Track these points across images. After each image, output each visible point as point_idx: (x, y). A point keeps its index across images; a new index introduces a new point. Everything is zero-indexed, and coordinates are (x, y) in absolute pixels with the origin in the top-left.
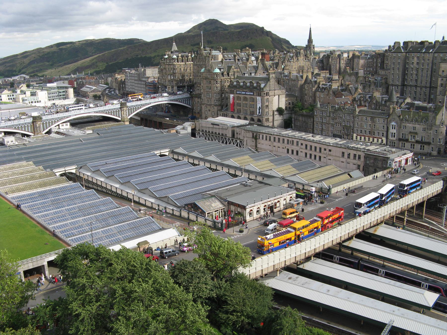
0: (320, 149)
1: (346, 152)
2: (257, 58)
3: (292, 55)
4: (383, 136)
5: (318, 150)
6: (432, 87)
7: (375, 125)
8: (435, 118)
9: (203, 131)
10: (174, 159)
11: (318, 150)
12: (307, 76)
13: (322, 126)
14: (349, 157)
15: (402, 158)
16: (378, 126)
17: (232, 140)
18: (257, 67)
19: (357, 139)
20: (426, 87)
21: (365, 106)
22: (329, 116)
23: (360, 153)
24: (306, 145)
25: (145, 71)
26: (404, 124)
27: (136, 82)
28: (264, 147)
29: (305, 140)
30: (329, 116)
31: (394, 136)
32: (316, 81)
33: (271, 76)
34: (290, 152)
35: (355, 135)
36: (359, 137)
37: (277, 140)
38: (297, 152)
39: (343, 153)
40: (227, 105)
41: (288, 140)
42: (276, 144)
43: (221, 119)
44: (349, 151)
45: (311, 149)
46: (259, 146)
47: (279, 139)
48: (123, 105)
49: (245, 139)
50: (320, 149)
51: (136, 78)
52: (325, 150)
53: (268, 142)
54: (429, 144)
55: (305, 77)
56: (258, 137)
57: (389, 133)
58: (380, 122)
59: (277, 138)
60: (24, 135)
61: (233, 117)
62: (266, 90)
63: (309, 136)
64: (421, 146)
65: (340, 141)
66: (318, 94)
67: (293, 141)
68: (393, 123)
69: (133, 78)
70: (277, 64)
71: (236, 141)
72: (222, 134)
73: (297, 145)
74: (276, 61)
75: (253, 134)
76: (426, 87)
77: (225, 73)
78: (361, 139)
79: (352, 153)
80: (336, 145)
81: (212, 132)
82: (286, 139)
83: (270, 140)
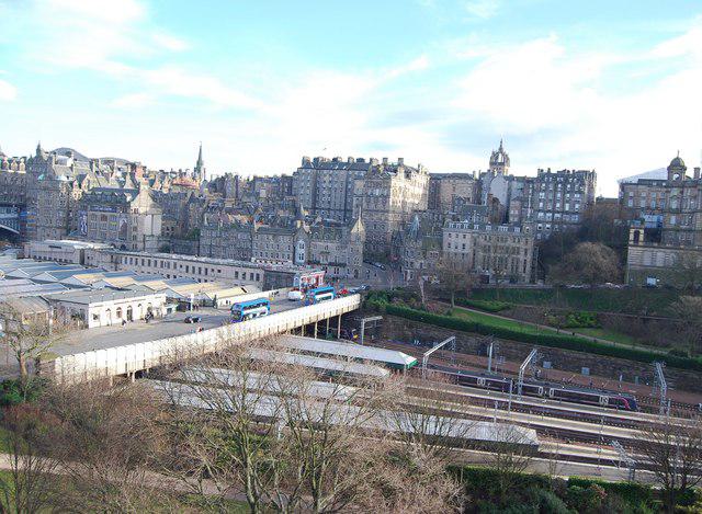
2: (124, 175)
3: (174, 176)
5: (203, 272)
6: (347, 210)
8: (349, 233)
11: (203, 272)
15: (313, 275)
18: (124, 182)
20: (340, 210)
37: (146, 263)
39: (237, 273)
42: (145, 268)
44: (245, 270)
45: (194, 272)
54: (344, 265)
58: (285, 241)
62: (134, 206)
73: (175, 267)
74: (152, 178)
76: (340, 210)
77: (76, 183)
79: (248, 271)
82: (159, 261)
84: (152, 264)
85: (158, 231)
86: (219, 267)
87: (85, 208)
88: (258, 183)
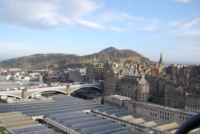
0: (168, 113)
1: (182, 116)
2: (135, 67)
3: (152, 66)
5: (167, 114)
9: (107, 101)
10: (112, 121)
11: (167, 114)
12: (160, 77)
14: (184, 119)
17: (122, 107)
18: (135, 71)
19: (187, 109)
21: (191, 92)
24: (161, 111)
25: (79, 70)
27: (74, 75)
28: (138, 111)
29: (160, 109)
32: (165, 79)
33: (142, 76)
34: (152, 114)
35: (186, 107)
36: (188, 108)
37: (145, 108)
38: (156, 114)
39: (181, 116)
40: (120, 89)
41: (151, 108)
43: (116, 96)
44: (184, 115)
45: (163, 114)
46: (136, 110)
48: (68, 86)
49: (129, 107)
50: (168, 113)
51: (75, 74)
52: (171, 114)
53: (141, 109)
55: (159, 77)
56: (136, 106)
60: (17, 98)
61: (122, 95)
62: (140, 83)
63: (162, 107)
65: (178, 110)
66: (166, 85)
67: (154, 109)
69: (73, 73)
70: (145, 70)
71: (124, 108)
72: (117, 104)
73: (156, 111)
74: (145, 68)
77: (120, 73)
78: (194, 110)
81: (112, 103)
82: (150, 108)
84: (148, 109)
85: (148, 91)
87: (123, 83)
88: (185, 69)
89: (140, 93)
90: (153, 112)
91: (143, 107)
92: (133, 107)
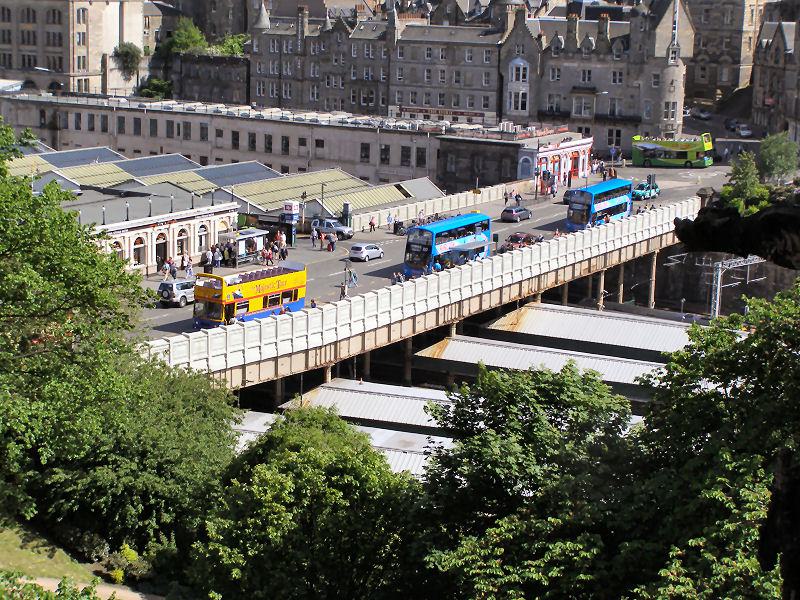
0: (286, 141)
4: (486, 106)
7: (458, 74)
8: (650, 35)
13: (279, 89)
14: (385, 160)
16: (469, 75)
22: (304, 54)
23: (421, 142)
24: (236, 136)
26: (552, 63)
30: (304, 54)
31: (524, 107)
39: (365, 148)
41: (170, 124)
47: (137, 122)
50: (286, 141)
56: (60, 123)
57: (506, 95)
59: (129, 118)
64: (611, 133)
67: (187, 126)
68: (521, 63)
73: (204, 137)
75: (42, 114)
80: (342, 127)
83: (105, 129)
86: (319, 134)
89: (80, 51)
90: (186, 143)
91: (113, 125)
92: (46, 133)
